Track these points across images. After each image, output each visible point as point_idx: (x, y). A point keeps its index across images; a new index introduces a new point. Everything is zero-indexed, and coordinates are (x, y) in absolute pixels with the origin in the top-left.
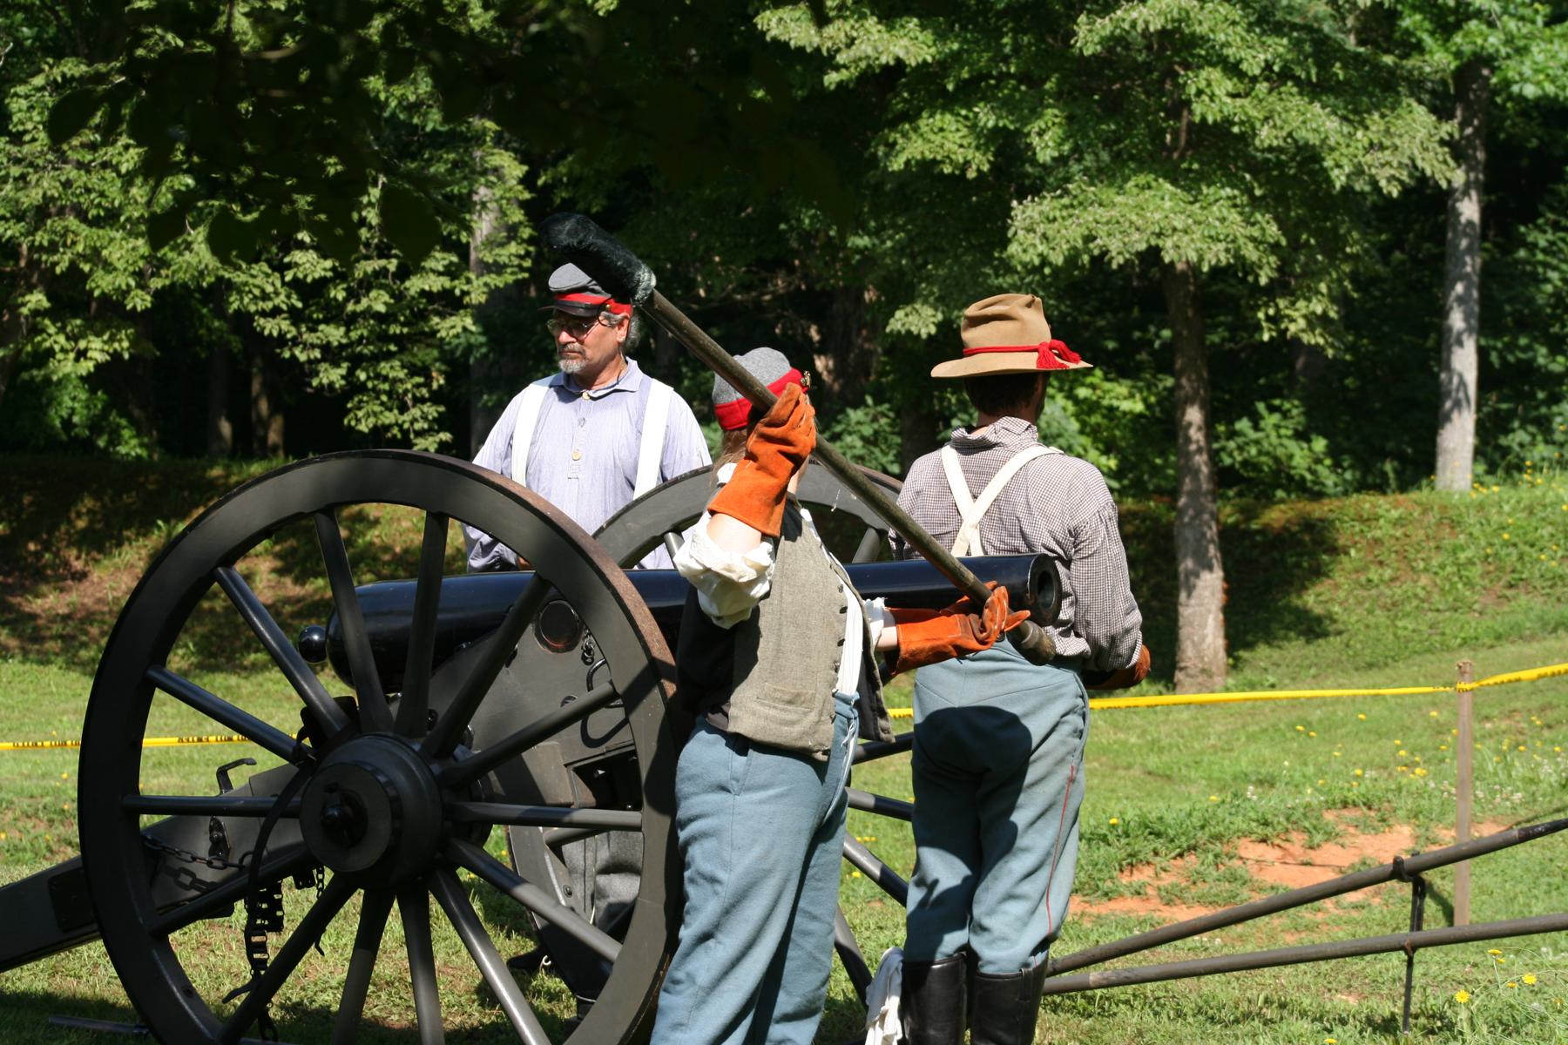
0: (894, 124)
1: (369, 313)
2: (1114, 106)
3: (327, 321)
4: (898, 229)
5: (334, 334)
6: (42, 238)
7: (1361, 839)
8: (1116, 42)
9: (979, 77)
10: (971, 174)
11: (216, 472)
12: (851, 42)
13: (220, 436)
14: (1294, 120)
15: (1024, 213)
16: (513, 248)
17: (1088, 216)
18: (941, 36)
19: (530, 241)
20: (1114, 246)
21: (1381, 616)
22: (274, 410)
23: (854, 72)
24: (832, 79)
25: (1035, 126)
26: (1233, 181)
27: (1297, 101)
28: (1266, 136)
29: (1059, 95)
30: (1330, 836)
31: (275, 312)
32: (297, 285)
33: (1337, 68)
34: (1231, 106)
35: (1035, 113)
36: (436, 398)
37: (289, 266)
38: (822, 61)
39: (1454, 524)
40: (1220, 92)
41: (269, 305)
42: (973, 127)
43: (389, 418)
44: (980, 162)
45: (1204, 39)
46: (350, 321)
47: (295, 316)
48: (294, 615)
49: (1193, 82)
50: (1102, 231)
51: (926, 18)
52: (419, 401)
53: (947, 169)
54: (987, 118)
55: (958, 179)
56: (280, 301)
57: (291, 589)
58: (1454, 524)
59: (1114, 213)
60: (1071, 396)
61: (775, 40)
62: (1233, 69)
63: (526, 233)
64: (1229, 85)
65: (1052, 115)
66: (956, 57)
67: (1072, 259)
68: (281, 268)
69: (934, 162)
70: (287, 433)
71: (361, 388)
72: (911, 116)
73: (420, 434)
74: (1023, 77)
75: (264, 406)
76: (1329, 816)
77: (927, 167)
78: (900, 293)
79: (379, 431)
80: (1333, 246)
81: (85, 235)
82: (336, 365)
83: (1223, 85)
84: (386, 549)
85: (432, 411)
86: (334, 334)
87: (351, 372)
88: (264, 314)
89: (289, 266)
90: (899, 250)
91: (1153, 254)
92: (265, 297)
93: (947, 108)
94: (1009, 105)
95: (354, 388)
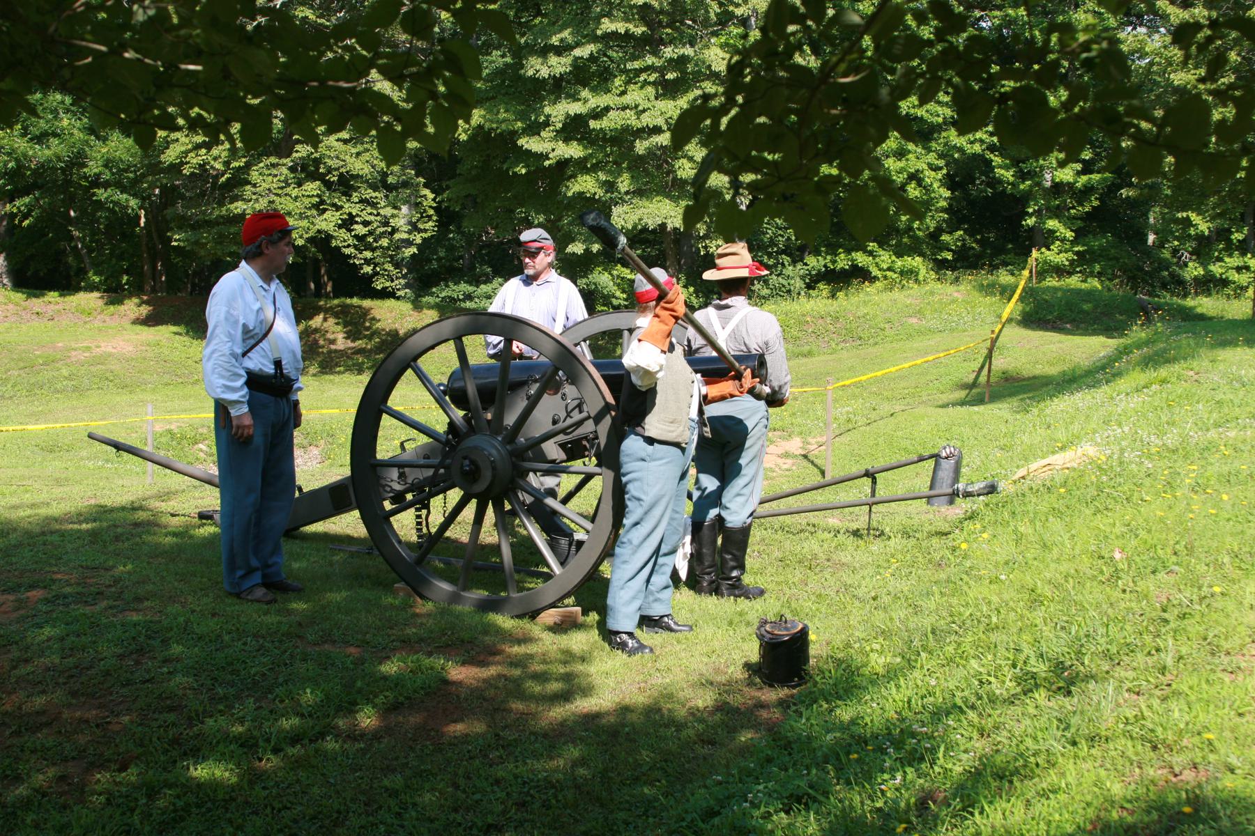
1: (381, 247)
3: (365, 250)
4: (569, 216)
5: (368, 254)
7: (783, 443)
9: (599, 162)
10: (597, 197)
11: (322, 303)
12: (553, 150)
13: (310, 289)
15: (617, 211)
16: (431, 223)
17: (639, 212)
18: (585, 148)
19: (436, 221)
20: (650, 222)
22: (329, 280)
23: (554, 161)
24: (547, 163)
25: (620, 180)
29: (629, 169)
30: (772, 442)
31: (349, 246)
32: (356, 237)
35: (620, 175)
36: (404, 277)
37: (353, 230)
40: (687, 167)
41: (346, 244)
42: (597, 180)
43: (388, 284)
46: (373, 250)
47: (355, 247)
48: (352, 354)
50: (645, 216)
51: (579, 141)
52: (397, 278)
53: (588, 195)
56: (350, 242)
57: (350, 344)
59: (650, 210)
60: (610, 274)
61: (526, 149)
63: (435, 218)
64: (690, 165)
65: (626, 176)
66: (591, 155)
67: (635, 227)
68: (350, 230)
69: (583, 193)
70: (334, 287)
71: (377, 274)
72: (574, 176)
73: (398, 290)
74: (615, 163)
75: (326, 278)
77: (581, 194)
79: (384, 289)
82: (369, 265)
84: (383, 330)
85: (403, 281)
86: (368, 254)
87: (374, 268)
88: (344, 247)
89: (353, 230)
91: (663, 226)
92: (345, 241)
93: (587, 173)
94: (610, 172)
95: (376, 274)
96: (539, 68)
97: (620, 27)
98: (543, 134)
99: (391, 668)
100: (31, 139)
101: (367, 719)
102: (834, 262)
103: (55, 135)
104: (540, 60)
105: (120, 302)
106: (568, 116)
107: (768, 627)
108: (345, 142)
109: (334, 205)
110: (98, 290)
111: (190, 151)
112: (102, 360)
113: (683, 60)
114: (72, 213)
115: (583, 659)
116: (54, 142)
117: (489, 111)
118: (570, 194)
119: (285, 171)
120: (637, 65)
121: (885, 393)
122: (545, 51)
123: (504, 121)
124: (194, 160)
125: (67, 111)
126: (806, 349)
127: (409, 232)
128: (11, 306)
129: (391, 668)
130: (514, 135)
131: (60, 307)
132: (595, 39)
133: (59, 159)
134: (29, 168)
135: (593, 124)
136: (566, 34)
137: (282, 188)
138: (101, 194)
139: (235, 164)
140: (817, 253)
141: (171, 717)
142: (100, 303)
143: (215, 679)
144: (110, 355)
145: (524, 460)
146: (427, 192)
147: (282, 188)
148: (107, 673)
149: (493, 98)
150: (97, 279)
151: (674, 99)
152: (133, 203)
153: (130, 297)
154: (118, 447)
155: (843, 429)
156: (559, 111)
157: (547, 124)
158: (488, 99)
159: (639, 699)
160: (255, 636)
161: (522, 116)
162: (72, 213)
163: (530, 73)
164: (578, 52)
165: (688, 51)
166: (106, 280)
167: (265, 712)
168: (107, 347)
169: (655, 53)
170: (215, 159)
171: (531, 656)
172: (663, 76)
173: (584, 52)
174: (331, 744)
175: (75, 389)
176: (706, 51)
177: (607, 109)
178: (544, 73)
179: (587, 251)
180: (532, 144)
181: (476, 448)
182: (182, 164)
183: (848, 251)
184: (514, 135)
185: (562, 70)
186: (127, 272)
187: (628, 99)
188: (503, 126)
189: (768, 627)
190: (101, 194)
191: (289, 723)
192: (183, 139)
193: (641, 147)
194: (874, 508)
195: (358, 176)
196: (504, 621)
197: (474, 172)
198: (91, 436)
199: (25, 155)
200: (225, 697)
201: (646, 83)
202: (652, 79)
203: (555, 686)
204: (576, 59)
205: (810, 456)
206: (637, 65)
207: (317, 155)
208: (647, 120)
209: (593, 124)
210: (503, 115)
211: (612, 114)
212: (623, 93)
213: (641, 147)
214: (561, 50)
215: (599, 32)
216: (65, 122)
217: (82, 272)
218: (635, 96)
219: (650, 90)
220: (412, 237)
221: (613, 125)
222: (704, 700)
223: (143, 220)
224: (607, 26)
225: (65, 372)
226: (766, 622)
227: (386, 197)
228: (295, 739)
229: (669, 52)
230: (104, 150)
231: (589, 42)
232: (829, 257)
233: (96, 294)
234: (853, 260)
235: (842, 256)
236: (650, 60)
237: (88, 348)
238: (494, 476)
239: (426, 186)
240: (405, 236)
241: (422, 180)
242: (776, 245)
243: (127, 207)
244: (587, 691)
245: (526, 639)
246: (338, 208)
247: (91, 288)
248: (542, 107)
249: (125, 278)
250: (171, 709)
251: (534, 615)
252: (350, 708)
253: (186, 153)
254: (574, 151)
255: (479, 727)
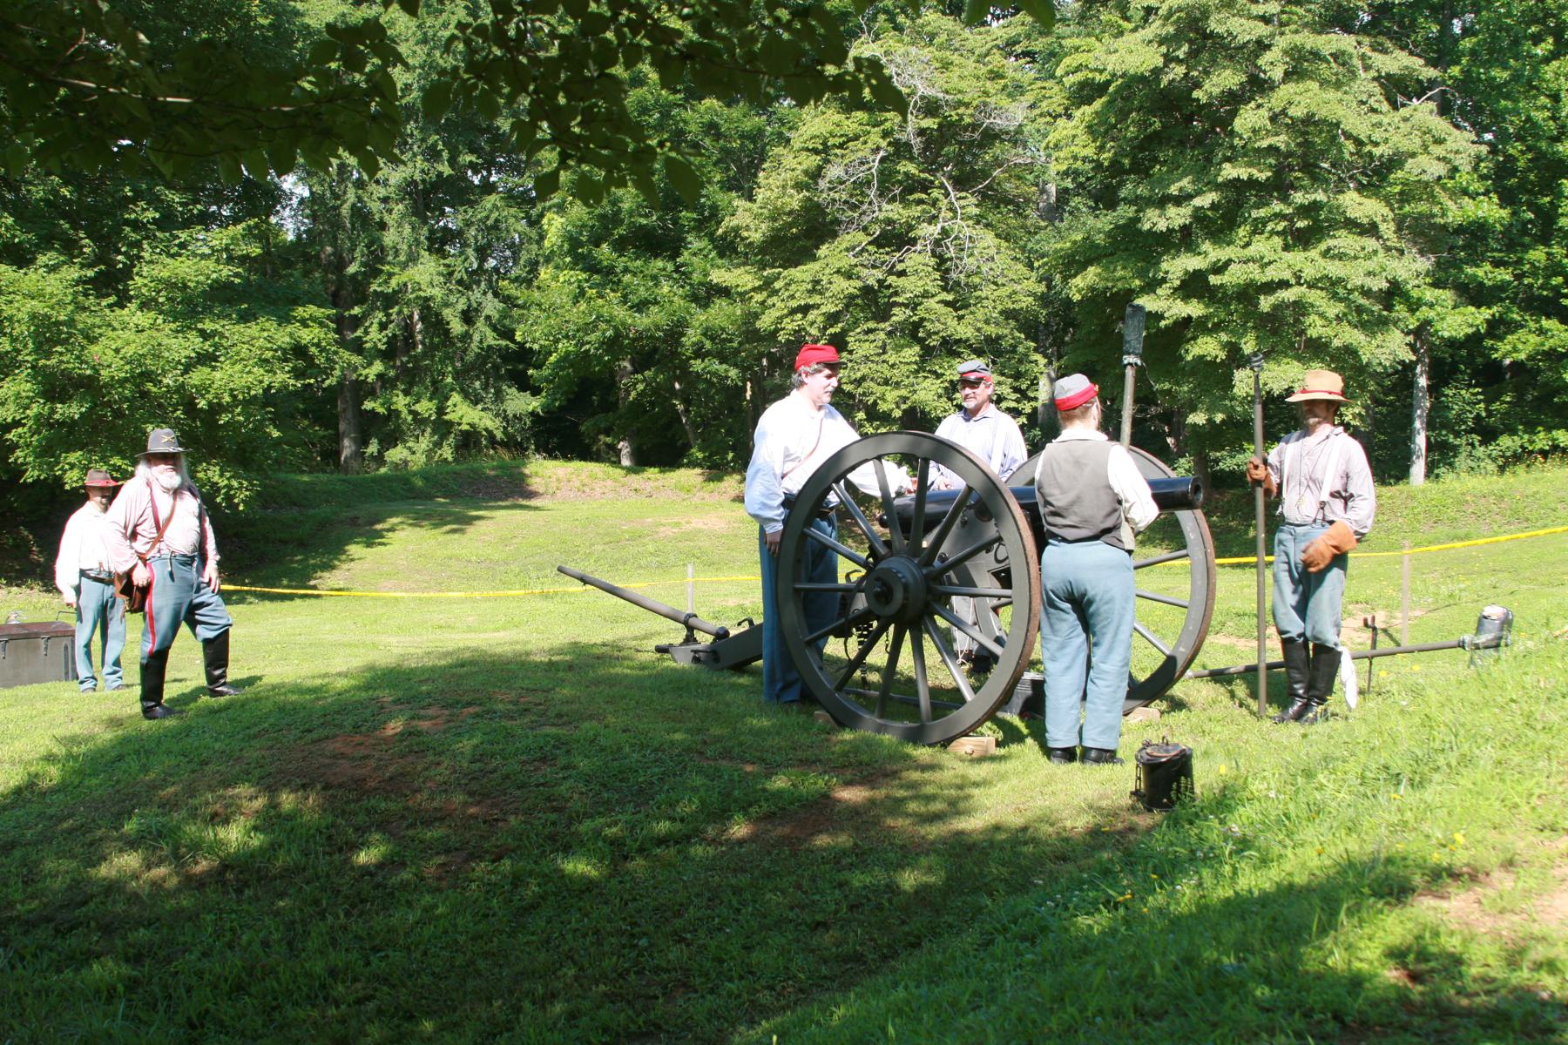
0: (1188, 341)
2: (1274, 332)
6: (860, 390)
8: (1275, 307)
14: (1347, 335)
18: (1207, 306)
21: (1383, 534)
24: (1163, 324)
26: (1323, 361)
27: (1348, 328)
28: (1336, 343)
33: (1365, 316)
34: (1322, 331)
38: (1159, 316)
39: (1413, 498)
44: (1222, 355)
45: (1312, 306)
49: (1308, 320)
51: (1200, 298)
54: (1224, 337)
55: (1213, 363)
58: (1413, 498)
62: (1322, 315)
72: (1195, 338)
76: (1350, 607)
78: (1193, 409)
80: (1363, 387)
81: (878, 390)
83: (1319, 322)
90: (1191, 391)
96: (1157, 221)
97: (1242, 172)
98: (1159, 291)
99: (780, 783)
100: (631, 307)
101: (740, 829)
102: (1531, 442)
103: (656, 303)
104: (1157, 212)
105: (720, 479)
106: (1187, 272)
107: (1149, 750)
108: (947, 303)
109: (935, 373)
110: (699, 465)
111: (786, 316)
112: (692, 536)
113: (1315, 206)
114: (677, 386)
115: (976, 785)
116: (653, 309)
117: (1106, 269)
118: (1189, 358)
119: (882, 335)
120: (1262, 213)
121: (1541, 579)
122: (1162, 202)
123: (1120, 279)
124: (790, 325)
125: (670, 277)
126: (1462, 532)
127: (1017, 401)
128: (609, 483)
129: (780, 783)
130: (1130, 294)
131: (660, 483)
132: (1218, 187)
133: (658, 328)
134: (627, 337)
135: (1214, 280)
136: (1186, 183)
137: (879, 355)
138: (697, 365)
139: (832, 331)
140: (1512, 432)
141: (553, 816)
142: (701, 479)
143: (604, 785)
144: (700, 531)
145: (942, 584)
146: (1038, 357)
147: (879, 355)
148: (507, 777)
149: (1112, 254)
150: (700, 455)
151: (1305, 250)
152: (733, 373)
153: (730, 474)
154: (584, 580)
155: (1441, 603)
156: (1177, 266)
157: (1164, 280)
158: (1105, 256)
159: (1016, 821)
160: (656, 750)
161: (1141, 274)
162: (677, 386)
163: (1146, 227)
164: (1197, 202)
165: (1320, 196)
166: (711, 455)
167: (641, 816)
168: (697, 522)
169: (1285, 199)
170: (812, 324)
171: (925, 783)
172: (1292, 223)
173: (1205, 200)
174: (698, 851)
175: (660, 565)
176: (1340, 197)
177: (1229, 262)
178: (1162, 226)
179: (1210, 421)
180: (1148, 303)
181: (889, 570)
182: (777, 331)
183: (1549, 429)
184: (1130, 294)
185: (1181, 221)
186: (733, 449)
187: (1252, 251)
188: (1120, 285)
189: (1149, 750)
190: (697, 365)
191: (663, 827)
192: (779, 304)
193: (1265, 303)
194: (1375, 660)
195: (959, 341)
196: (923, 753)
197: (1092, 338)
198: (561, 570)
199: (623, 324)
200: (608, 802)
201: (1273, 233)
202: (1280, 228)
203: (938, 806)
204: (1197, 209)
205: (1391, 631)
206: (1262, 213)
207: (915, 318)
208: (1272, 274)
209: (1214, 280)
210: (1120, 273)
211: (1232, 267)
212: (1248, 244)
213: (1265, 303)
214: (1179, 201)
215: (1220, 179)
216: (666, 289)
217: (688, 446)
218: (1262, 246)
219: (1277, 241)
220: (1021, 406)
221: (1235, 280)
222: (1080, 823)
223: (749, 394)
224: (1229, 172)
225: (651, 548)
226: (1148, 745)
227: (994, 362)
228: (662, 841)
229: (1299, 198)
230: (703, 318)
231: (1210, 190)
232: (1526, 437)
233: (698, 470)
234: (1554, 440)
235: (1542, 435)
236: (1277, 207)
237: (678, 524)
238: (906, 598)
239: (1036, 350)
240: (1013, 405)
241: (1033, 344)
242: (1465, 423)
243: (727, 377)
244: (967, 812)
245: (932, 767)
246: (938, 376)
247: (693, 464)
248: (1158, 263)
249: (730, 455)
250: (555, 810)
251: (946, 743)
252: (722, 815)
253: (781, 318)
254: (1195, 309)
255: (844, 840)
